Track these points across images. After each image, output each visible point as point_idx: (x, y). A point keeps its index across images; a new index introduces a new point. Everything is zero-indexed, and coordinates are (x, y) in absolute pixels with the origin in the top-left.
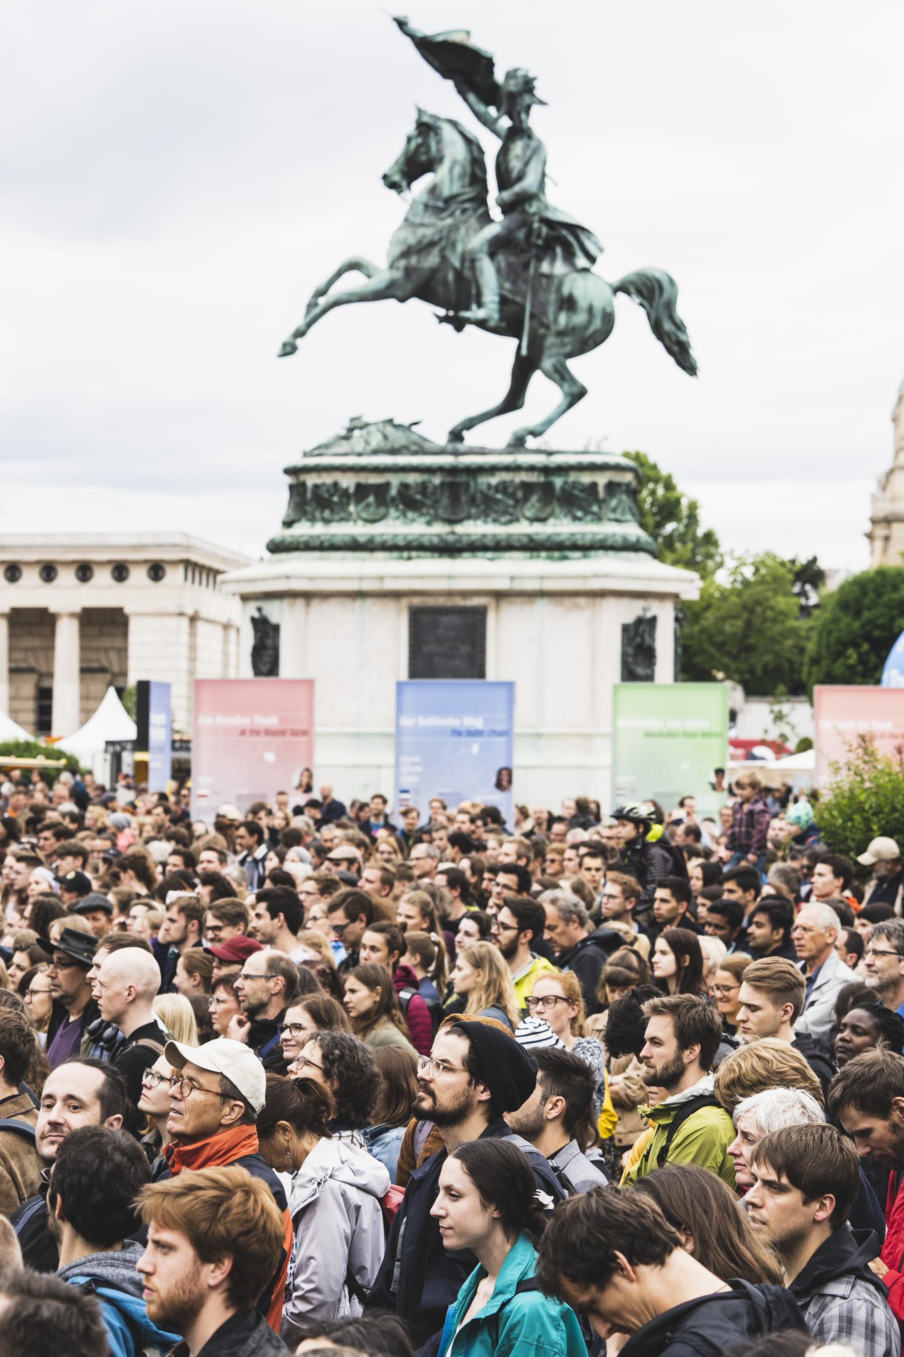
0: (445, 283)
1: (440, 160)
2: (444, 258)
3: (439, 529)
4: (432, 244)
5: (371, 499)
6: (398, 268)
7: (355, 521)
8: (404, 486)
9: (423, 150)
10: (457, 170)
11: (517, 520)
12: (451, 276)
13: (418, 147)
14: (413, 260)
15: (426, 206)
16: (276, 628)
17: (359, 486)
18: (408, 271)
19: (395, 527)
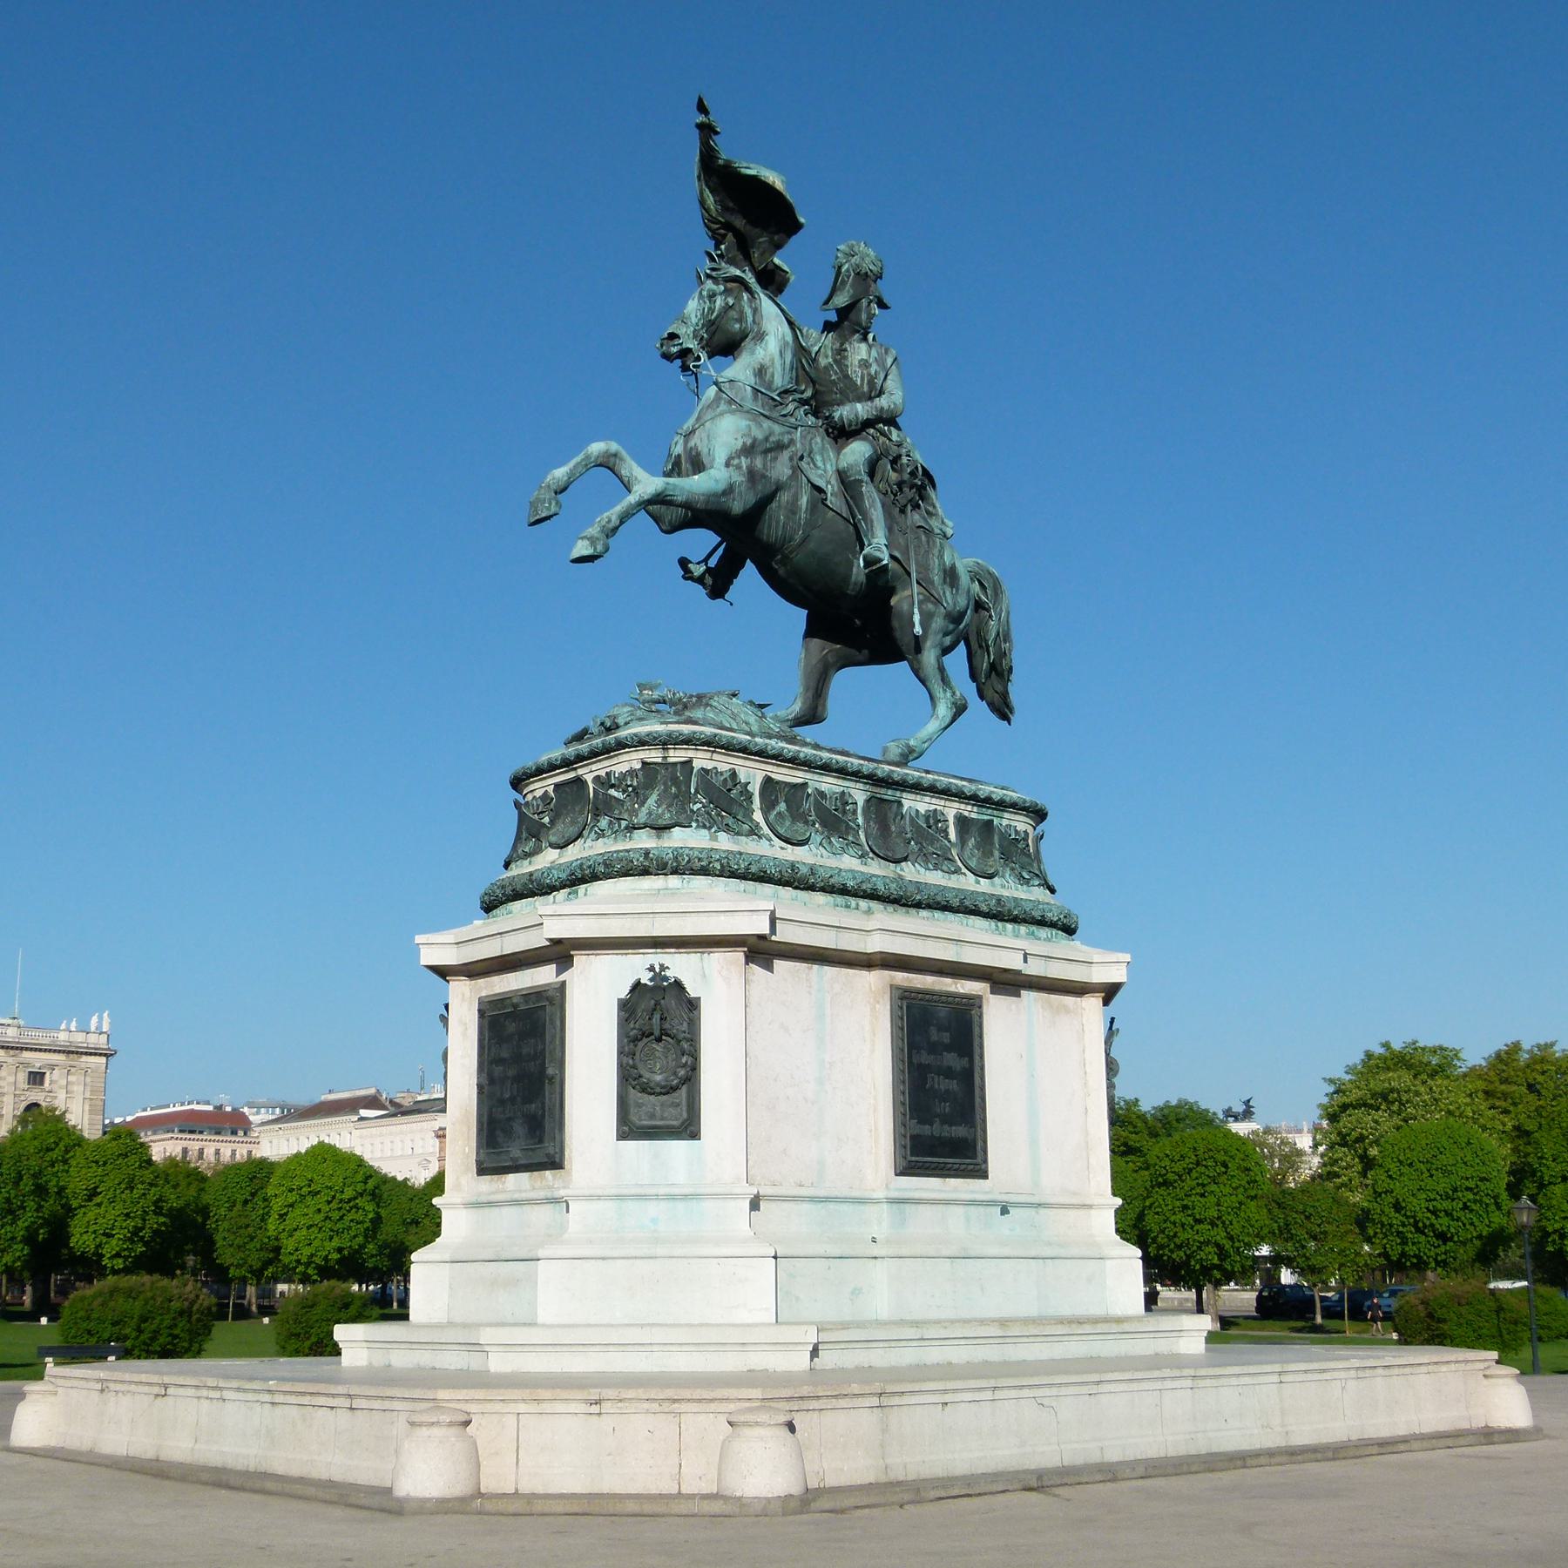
0: (793, 509)
1: (760, 337)
2: (797, 470)
3: (876, 869)
4: (780, 447)
5: (782, 807)
6: (739, 467)
7: (770, 840)
8: (822, 794)
9: (733, 314)
10: (789, 357)
11: (957, 871)
12: (804, 501)
13: (728, 308)
14: (758, 463)
15: (756, 391)
16: (693, 1005)
17: (768, 782)
18: (753, 476)
19: (810, 856)
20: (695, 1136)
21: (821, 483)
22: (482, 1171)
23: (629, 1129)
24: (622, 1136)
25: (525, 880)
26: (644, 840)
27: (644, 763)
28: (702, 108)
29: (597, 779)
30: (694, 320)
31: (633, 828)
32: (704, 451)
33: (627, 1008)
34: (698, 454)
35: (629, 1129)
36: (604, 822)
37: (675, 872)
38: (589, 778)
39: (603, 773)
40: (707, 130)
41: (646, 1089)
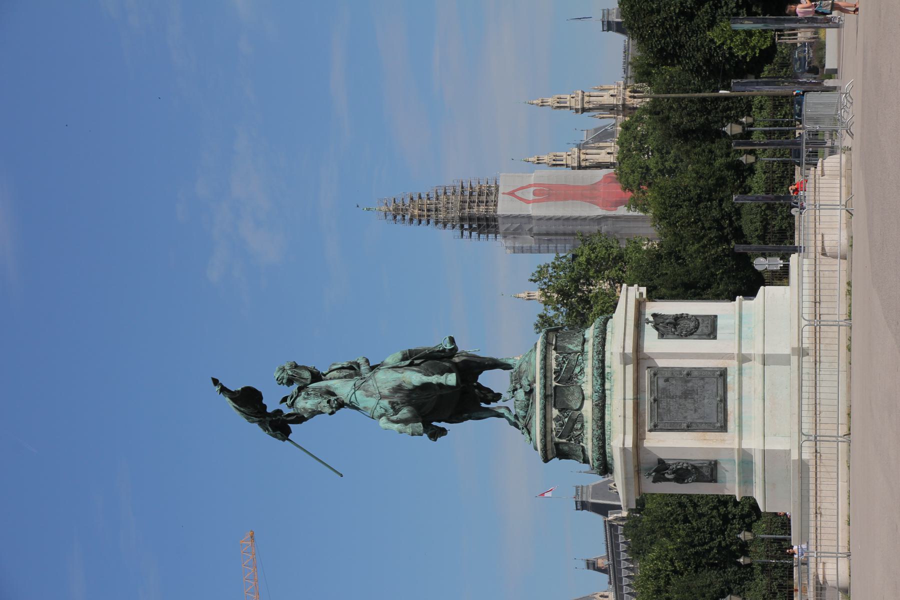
1: (327, 386)
20: (716, 316)
21: (408, 362)
22: (724, 428)
23: (712, 334)
24: (715, 338)
25: (596, 410)
26: (589, 347)
27: (555, 349)
28: (216, 382)
29: (555, 379)
30: (320, 400)
31: (583, 352)
32: (394, 384)
33: (662, 336)
34: (393, 388)
35: (712, 334)
36: (577, 370)
37: (606, 330)
38: (554, 384)
39: (554, 376)
40: (224, 390)
41: (697, 328)
